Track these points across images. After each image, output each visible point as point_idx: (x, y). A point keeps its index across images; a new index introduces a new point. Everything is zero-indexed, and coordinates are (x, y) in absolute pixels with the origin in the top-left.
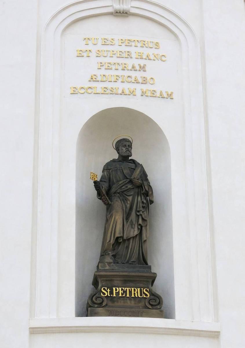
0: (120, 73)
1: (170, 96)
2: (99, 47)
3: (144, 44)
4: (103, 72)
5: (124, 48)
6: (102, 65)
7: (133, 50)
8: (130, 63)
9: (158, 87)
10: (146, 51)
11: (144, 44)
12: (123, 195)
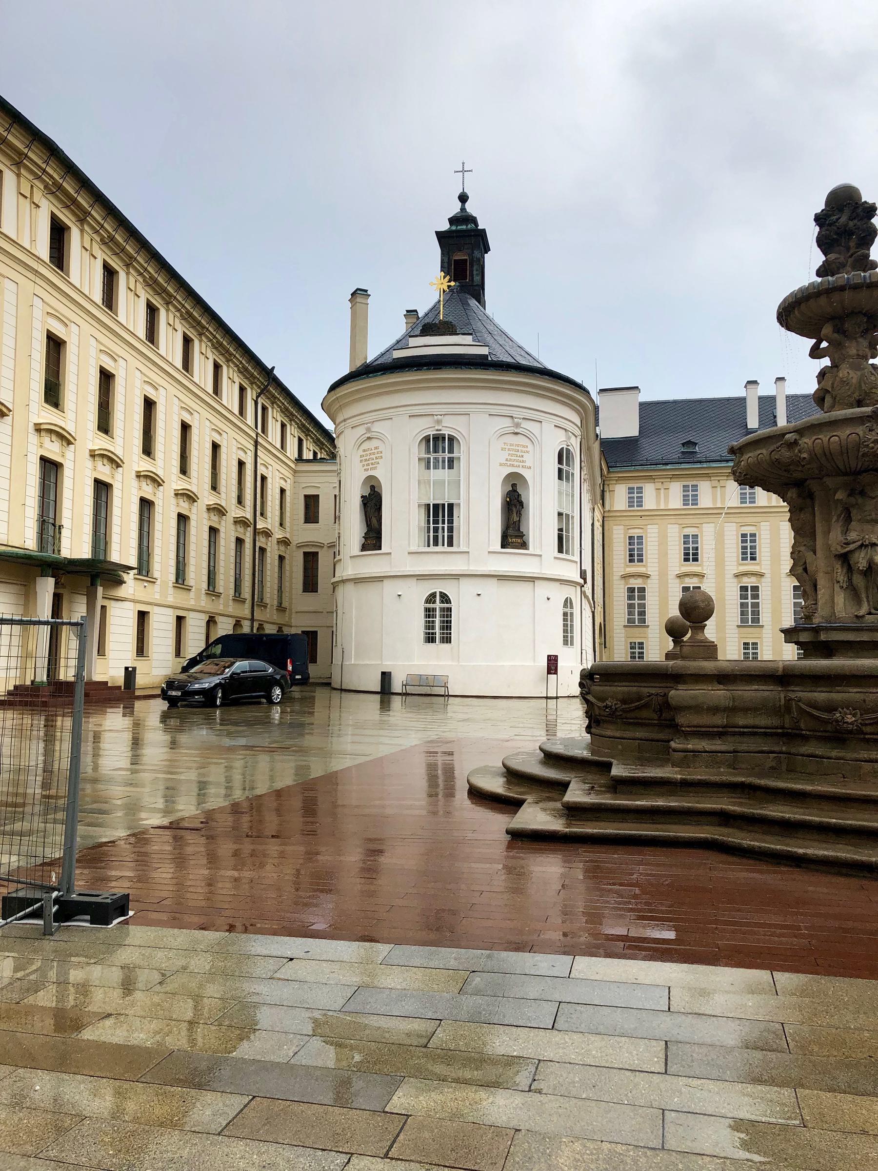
0: (515, 458)
1: (530, 467)
3: (524, 446)
4: (510, 457)
7: (520, 449)
8: (519, 454)
9: (527, 464)
11: (524, 446)
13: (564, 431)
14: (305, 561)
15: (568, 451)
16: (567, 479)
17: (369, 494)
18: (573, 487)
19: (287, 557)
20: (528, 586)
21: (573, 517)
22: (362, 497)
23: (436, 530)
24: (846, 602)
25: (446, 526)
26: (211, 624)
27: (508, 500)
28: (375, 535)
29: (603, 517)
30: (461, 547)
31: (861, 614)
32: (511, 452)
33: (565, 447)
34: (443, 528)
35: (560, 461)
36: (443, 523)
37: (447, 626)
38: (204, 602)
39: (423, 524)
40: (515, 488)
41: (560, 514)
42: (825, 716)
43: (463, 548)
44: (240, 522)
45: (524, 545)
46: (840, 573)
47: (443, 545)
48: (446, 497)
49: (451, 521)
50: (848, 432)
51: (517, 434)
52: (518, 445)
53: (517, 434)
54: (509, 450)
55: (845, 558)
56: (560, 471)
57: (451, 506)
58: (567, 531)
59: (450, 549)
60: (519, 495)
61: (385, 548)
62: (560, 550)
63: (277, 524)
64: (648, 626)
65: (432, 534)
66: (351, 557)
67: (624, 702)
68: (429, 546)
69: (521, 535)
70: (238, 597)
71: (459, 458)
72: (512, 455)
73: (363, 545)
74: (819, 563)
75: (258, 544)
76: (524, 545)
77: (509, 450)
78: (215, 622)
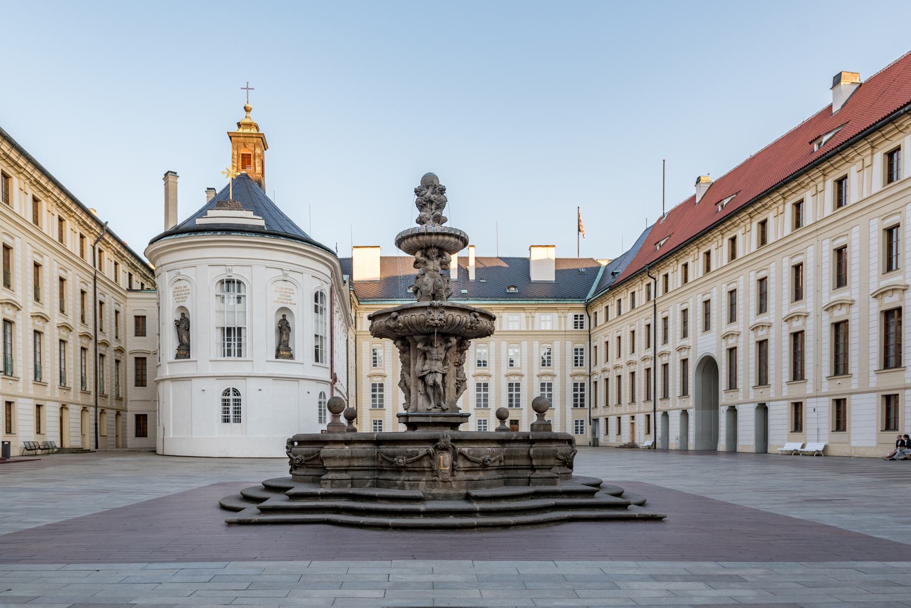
2: (280, 290)
3: (290, 289)
5: (285, 290)
6: (280, 294)
7: (287, 291)
8: (287, 294)
9: (293, 302)
10: (290, 291)
12: (285, 330)
13: (318, 280)
14: (136, 364)
15: (322, 294)
16: (321, 313)
17: (181, 319)
18: (325, 318)
19: (122, 361)
20: (294, 384)
21: (325, 338)
22: (175, 321)
23: (229, 345)
24: (424, 401)
25: (236, 342)
26: (64, 410)
27: (280, 326)
28: (186, 348)
29: (356, 336)
30: (247, 357)
31: (429, 408)
32: (282, 293)
33: (319, 290)
34: (234, 344)
35: (316, 300)
36: (234, 340)
37: (238, 411)
38: (58, 394)
39: (220, 341)
40: (284, 318)
41: (316, 336)
42: (391, 459)
43: (248, 358)
44: (85, 336)
45: (291, 357)
46: (421, 386)
47: (235, 356)
48: (236, 323)
49: (240, 340)
50: (419, 314)
51: (286, 281)
52: (286, 289)
53: (286, 281)
54: (280, 292)
55: (422, 378)
56: (316, 307)
57: (240, 329)
58: (322, 347)
59: (240, 359)
60: (287, 323)
61: (191, 359)
62: (317, 360)
63: (114, 337)
64: (385, 409)
65: (226, 348)
66: (168, 363)
67: (306, 456)
68: (224, 356)
69: (289, 350)
70: (84, 391)
71: (245, 296)
72: (282, 295)
73: (177, 354)
74: (411, 381)
75: (98, 352)
76: (291, 357)
77: (280, 292)
78: (67, 409)
